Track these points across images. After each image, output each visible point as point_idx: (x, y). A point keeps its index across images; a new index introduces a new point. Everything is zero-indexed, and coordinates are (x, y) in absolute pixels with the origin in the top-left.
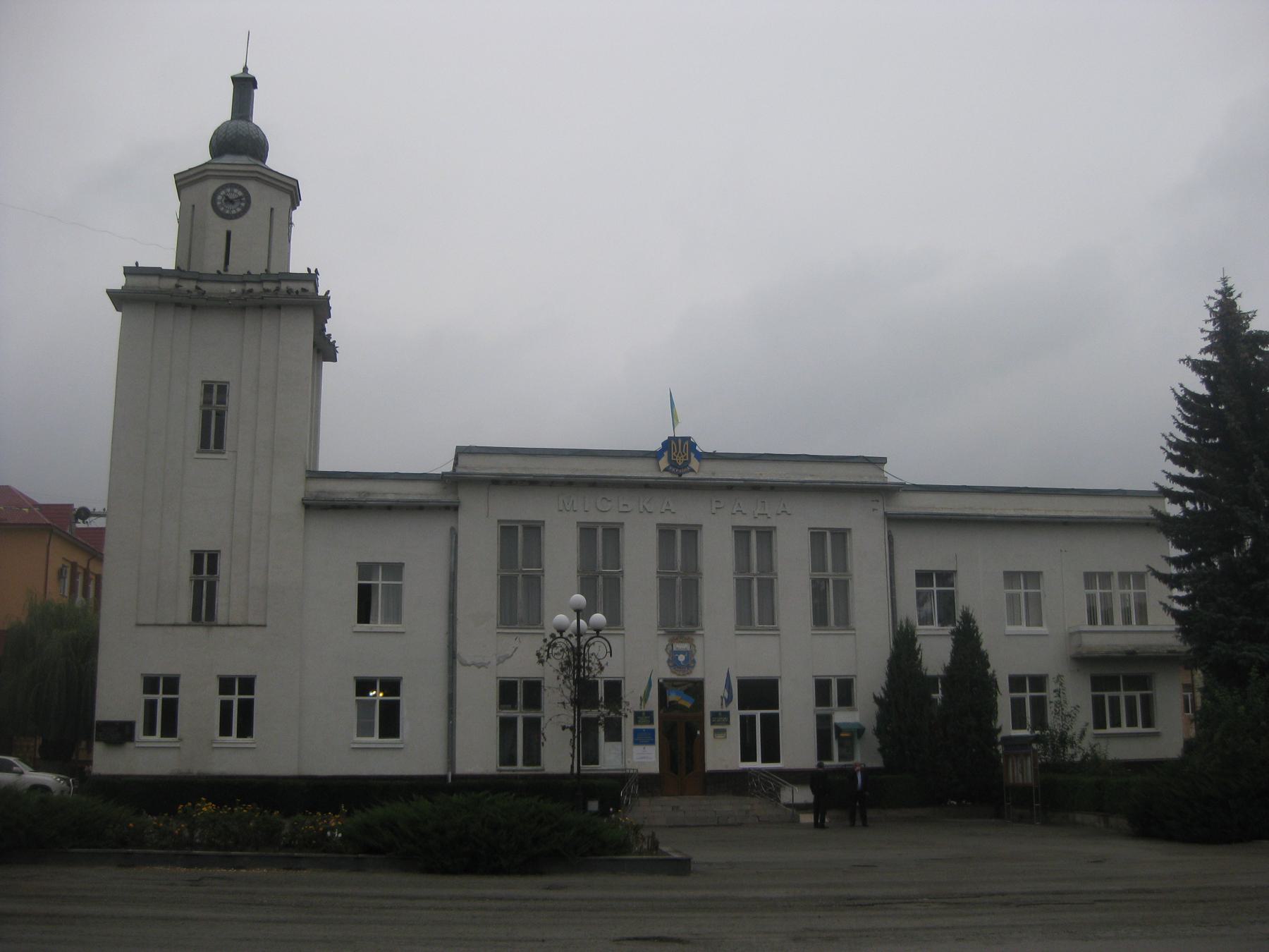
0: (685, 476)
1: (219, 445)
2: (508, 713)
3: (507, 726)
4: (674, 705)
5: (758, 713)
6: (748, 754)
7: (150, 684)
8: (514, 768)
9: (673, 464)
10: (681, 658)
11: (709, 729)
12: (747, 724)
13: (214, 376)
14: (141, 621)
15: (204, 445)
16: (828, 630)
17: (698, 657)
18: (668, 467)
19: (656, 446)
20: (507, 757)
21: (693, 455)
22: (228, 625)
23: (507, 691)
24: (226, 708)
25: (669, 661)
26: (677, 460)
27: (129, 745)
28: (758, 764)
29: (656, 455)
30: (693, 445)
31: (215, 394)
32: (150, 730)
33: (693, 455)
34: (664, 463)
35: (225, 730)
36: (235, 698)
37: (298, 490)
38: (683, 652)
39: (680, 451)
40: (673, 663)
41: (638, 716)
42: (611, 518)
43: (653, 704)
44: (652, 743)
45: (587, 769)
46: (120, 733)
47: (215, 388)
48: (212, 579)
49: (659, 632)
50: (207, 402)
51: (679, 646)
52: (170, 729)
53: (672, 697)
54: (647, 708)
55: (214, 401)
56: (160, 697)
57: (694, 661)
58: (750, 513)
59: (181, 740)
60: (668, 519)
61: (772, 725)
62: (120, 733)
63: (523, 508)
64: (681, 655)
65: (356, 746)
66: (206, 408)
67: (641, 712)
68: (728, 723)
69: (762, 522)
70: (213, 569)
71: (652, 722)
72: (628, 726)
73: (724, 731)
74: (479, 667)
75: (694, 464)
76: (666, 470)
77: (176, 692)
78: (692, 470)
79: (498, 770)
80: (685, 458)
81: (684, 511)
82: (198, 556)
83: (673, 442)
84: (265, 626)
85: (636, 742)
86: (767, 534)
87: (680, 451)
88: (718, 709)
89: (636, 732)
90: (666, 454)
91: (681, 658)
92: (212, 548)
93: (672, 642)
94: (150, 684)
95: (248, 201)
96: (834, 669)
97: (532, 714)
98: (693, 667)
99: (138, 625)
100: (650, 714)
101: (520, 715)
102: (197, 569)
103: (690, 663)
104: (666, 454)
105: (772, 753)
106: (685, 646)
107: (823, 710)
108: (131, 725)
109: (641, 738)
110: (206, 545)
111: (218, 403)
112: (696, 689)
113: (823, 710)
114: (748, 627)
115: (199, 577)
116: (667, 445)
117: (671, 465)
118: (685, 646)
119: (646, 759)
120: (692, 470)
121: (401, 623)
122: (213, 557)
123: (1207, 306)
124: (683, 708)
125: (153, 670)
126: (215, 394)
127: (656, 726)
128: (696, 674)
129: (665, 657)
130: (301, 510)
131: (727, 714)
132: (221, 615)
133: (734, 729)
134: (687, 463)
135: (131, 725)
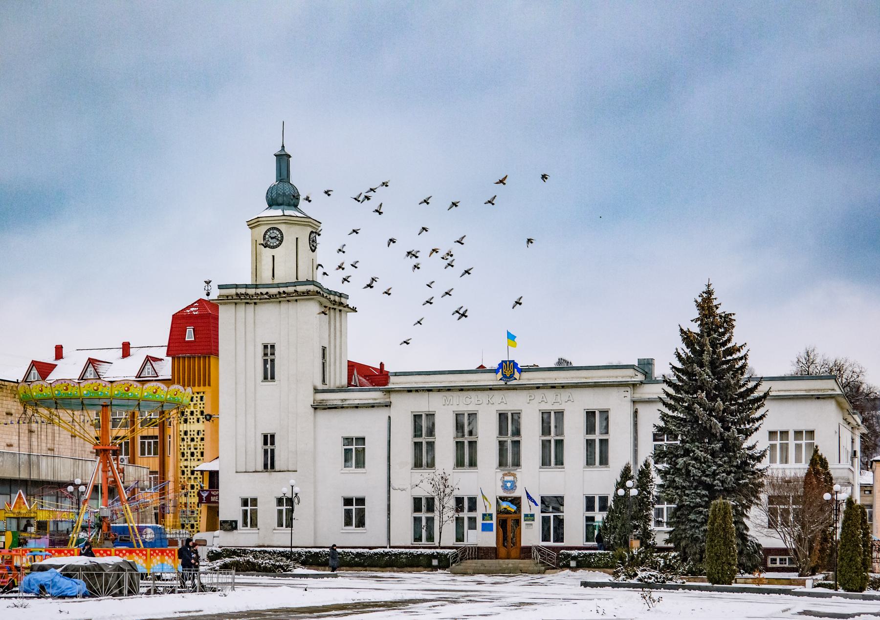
0: (508, 383)
1: (273, 378)
2: (417, 515)
3: (417, 520)
4: (507, 512)
5: (552, 515)
6: (545, 538)
7: (245, 502)
8: (420, 543)
9: (504, 376)
10: (509, 485)
11: (523, 523)
12: (545, 520)
13: (269, 341)
14: (238, 471)
15: (265, 378)
16: (595, 468)
17: (518, 484)
18: (502, 378)
19: (496, 366)
20: (418, 538)
21: (516, 370)
22: (280, 471)
23: (417, 504)
24: (280, 512)
25: (502, 486)
26: (506, 373)
27: (235, 531)
28: (551, 543)
29: (496, 371)
30: (515, 365)
31: (269, 350)
32: (245, 524)
33: (516, 370)
34: (500, 375)
35: (280, 524)
36: (284, 508)
37: (309, 398)
38: (510, 482)
39: (508, 368)
40: (505, 487)
41: (484, 515)
42: (471, 408)
43: (493, 510)
44: (492, 530)
45: (460, 544)
46: (231, 526)
47: (269, 347)
48: (272, 448)
49: (497, 470)
50: (266, 355)
51: (507, 478)
52: (254, 524)
53: (504, 505)
54: (489, 512)
55: (269, 354)
56: (249, 508)
57: (516, 486)
58: (550, 401)
59: (258, 529)
60: (503, 408)
61: (560, 522)
62: (231, 526)
63: (422, 404)
64: (509, 483)
65: (344, 531)
66: (265, 358)
67: (486, 514)
68: (533, 520)
69: (557, 407)
70: (273, 443)
71: (491, 519)
72: (479, 522)
73: (532, 524)
74: (402, 491)
75: (517, 375)
76: (501, 379)
77: (256, 505)
78: (516, 379)
79: (413, 544)
80: (511, 372)
81: (512, 402)
82: (265, 437)
83: (504, 364)
84: (297, 471)
85: (483, 530)
86: (560, 414)
87: (508, 368)
88: (529, 513)
89: (482, 524)
90: (501, 370)
91: (509, 485)
92: (272, 432)
93: (505, 475)
94: (245, 502)
95: (281, 241)
96: (597, 492)
97: (430, 515)
98: (515, 489)
99: (237, 472)
100: (491, 515)
101: (423, 515)
102: (265, 443)
103: (514, 487)
104: (501, 370)
105: (559, 538)
106: (511, 478)
107: (590, 514)
108: (236, 522)
109: (486, 528)
110: (269, 431)
111: (271, 355)
112: (516, 501)
113: (590, 514)
114: (548, 467)
115: (266, 447)
116: (501, 365)
117: (504, 377)
118: (511, 478)
119: (489, 539)
120: (516, 379)
121: (364, 467)
122: (273, 436)
123: (696, 301)
124: (508, 512)
125: (245, 496)
126: (269, 350)
127: (494, 522)
128: (516, 494)
129: (500, 484)
130: (312, 410)
131: (533, 515)
132: (277, 467)
133: (538, 523)
134: (512, 377)
135: (236, 522)
